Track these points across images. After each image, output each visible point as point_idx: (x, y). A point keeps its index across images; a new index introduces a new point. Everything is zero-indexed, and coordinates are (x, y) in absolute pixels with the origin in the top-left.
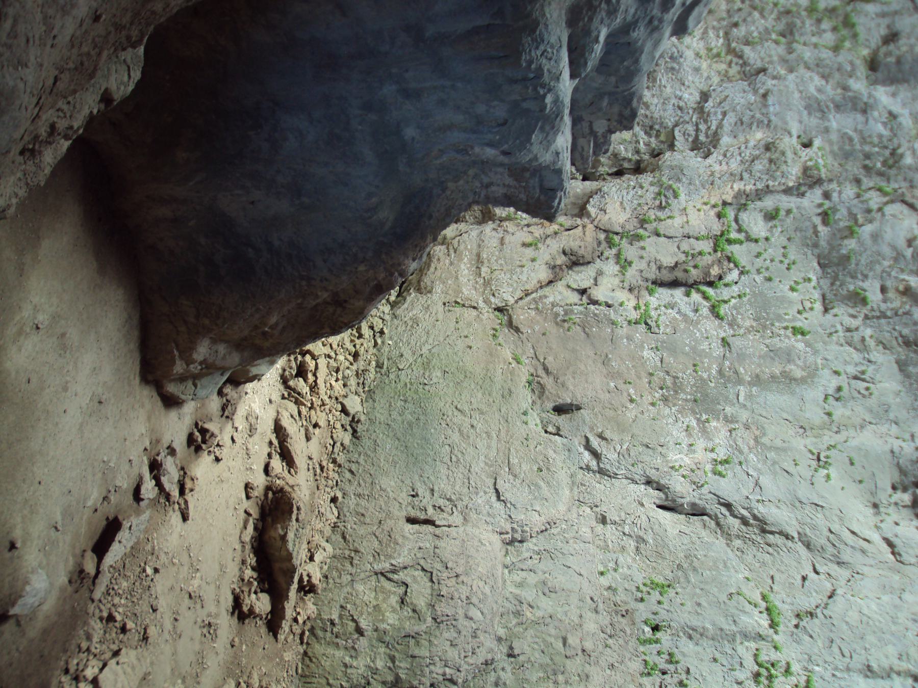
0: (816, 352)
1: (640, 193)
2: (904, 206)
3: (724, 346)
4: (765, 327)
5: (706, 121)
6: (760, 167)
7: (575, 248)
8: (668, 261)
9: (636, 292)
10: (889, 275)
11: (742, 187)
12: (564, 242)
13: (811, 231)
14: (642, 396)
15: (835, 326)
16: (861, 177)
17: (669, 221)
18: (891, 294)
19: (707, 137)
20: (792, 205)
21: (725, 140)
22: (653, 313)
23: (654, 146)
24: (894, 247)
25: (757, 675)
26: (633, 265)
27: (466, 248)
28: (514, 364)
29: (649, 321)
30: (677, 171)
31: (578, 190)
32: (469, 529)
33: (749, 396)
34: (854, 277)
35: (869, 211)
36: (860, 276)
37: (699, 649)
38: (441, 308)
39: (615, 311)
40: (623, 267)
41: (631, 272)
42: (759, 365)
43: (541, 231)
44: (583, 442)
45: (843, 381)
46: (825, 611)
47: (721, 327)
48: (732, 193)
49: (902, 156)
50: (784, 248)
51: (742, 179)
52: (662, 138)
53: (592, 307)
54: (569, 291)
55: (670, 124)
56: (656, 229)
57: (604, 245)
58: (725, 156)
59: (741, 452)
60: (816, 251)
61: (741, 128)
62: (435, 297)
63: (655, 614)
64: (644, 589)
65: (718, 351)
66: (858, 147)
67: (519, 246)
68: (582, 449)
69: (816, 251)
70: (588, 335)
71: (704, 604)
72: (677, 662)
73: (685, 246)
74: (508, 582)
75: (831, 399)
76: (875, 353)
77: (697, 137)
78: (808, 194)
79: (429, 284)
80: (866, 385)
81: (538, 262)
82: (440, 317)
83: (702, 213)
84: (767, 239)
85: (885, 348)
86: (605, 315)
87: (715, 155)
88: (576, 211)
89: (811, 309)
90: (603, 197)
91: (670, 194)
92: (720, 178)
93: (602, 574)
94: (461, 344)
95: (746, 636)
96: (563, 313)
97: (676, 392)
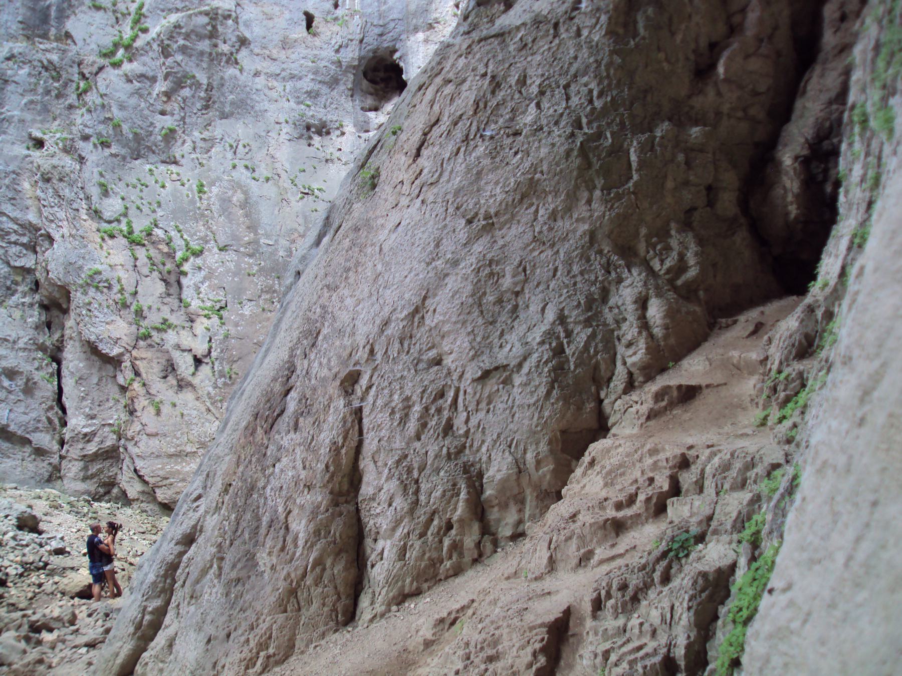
0: (219, 179)
1: (96, 306)
2: (99, 75)
3: (227, 250)
4: (203, 215)
5: (8, 233)
6: (67, 191)
7: (160, 367)
8: (160, 287)
9: (193, 317)
10: (152, 105)
11: (85, 211)
12: (155, 377)
13: (114, 159)
15: (193, 159)
16: (67, 103)
17: (123, 282)
18: (168, 108)
19: (24, 235)
20: (96, 170)
21: (32, 217)
22: (209, 304)
23: (26, 289)
24: (132, 94)
26: (166, 317)
27: (162, 469)
29: (217, 308)
30: (70, 268)
31: (81, 365)
33: (268, 236)
34: (151, 134)
35: (103, 106)
36: (151, 129)
39: (215, 335)
40: (169, 327)
41: (173, 319)
42: (238, 225)
43: (142, 399)
45: (240, 165)
47: (210, 250)
48: (90, 222)
49: (50, 62)
50: (128, 185)
51: (78, 210)
52: (19, 279)
53: (214, 354)
54: (199, 373)
55: (6, 270)
56: (131, 294)
57: (149, 341)
58: (52, 221)
60: (128, 159)
61: (19, 201)
65: (230, 256)
66: (39, 98)
67: (159, 419)
69: (128, 159)
70: (239, 358)
73: (145, 271)
75: (256, 175)
76: (215, 133)
77: (23, 245)
78: (83, 154)
80: (240, 147)
81: (176, 401)
83: (111, 251)
84: (123, 199)
85: (210, 125)
86: (220, 343)
87: (50, 231)
88: (110, 368)
89: (178, 174)
90: (101, 341)
91: (98, 278)
92: (78, 230)
96: (223, 379)
97: (275, 291)
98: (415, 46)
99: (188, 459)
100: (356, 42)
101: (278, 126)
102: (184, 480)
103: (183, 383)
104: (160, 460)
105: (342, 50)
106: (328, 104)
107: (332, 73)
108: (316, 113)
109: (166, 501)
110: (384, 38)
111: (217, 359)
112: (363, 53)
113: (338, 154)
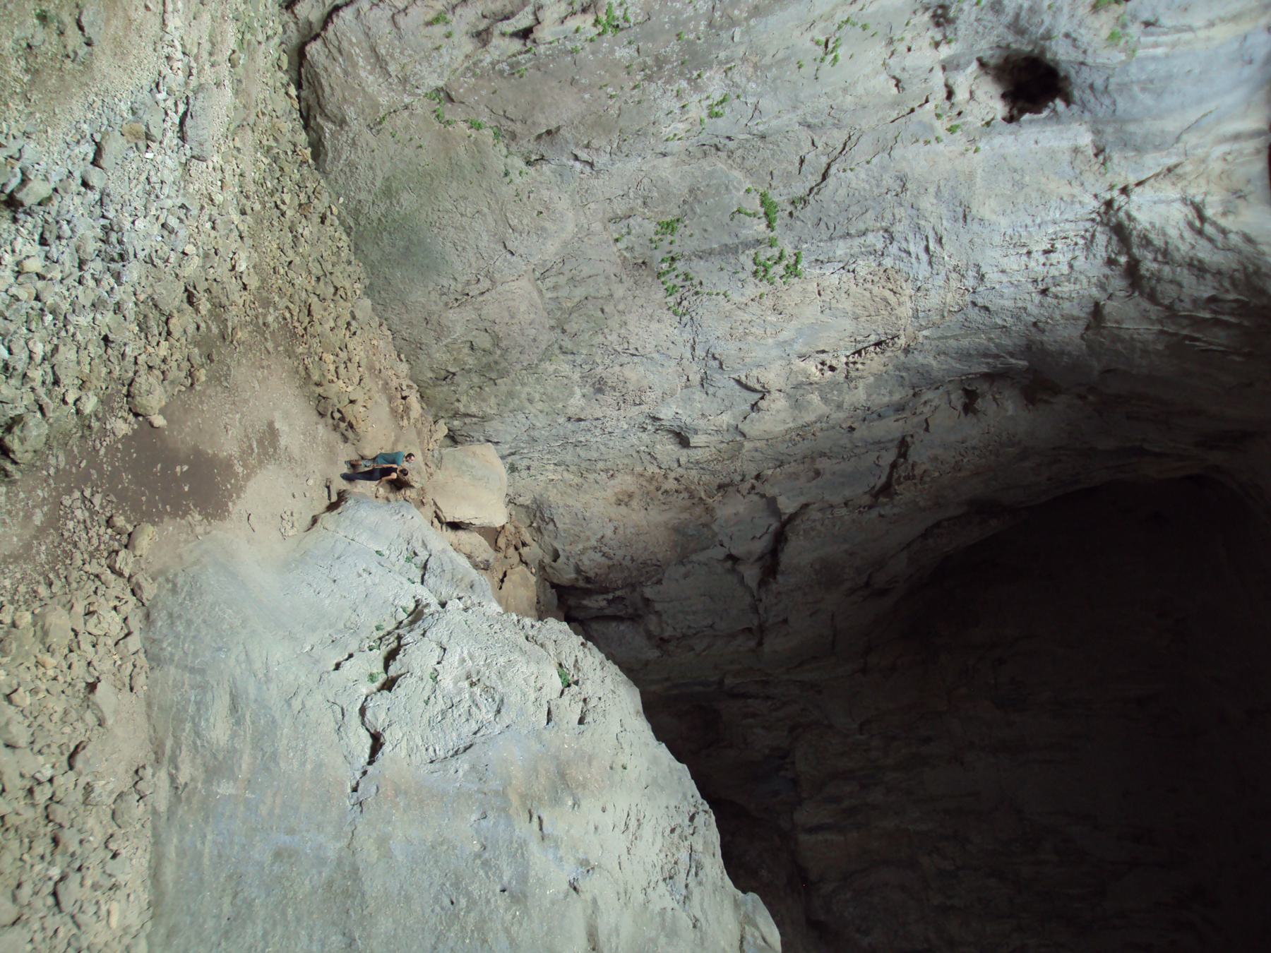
14: (622, 88)
25: (755, 273)
27: (351, 42)
28: (473, 133)
32: (500, 288)
37: (709, 264)
38: (368, 135)
46: (817, 197)
54: (507, 40)
59: (738, 86)
63: (670, 252)
64: (656, 238)
68: (572, 162)
71: (710, 229)
72: (691, 279)
74: (544, 291)
79: (335, 111)
82: (374, 144)
93: (617, 240)
94: (409, 152)
95: (747, 246)
96: (507, 68)
99: (378, 70)
100: (1081, 59)
102: (346, 73)
103: (484, 36)
104: (363, 37)
105: (1069, 41)
106: (983, 23)
107: (1033, 29)
109: (308, 57)
110: (1088, 91)
111: (535, 54)
112: (1064, 65)
113: (902, 48)
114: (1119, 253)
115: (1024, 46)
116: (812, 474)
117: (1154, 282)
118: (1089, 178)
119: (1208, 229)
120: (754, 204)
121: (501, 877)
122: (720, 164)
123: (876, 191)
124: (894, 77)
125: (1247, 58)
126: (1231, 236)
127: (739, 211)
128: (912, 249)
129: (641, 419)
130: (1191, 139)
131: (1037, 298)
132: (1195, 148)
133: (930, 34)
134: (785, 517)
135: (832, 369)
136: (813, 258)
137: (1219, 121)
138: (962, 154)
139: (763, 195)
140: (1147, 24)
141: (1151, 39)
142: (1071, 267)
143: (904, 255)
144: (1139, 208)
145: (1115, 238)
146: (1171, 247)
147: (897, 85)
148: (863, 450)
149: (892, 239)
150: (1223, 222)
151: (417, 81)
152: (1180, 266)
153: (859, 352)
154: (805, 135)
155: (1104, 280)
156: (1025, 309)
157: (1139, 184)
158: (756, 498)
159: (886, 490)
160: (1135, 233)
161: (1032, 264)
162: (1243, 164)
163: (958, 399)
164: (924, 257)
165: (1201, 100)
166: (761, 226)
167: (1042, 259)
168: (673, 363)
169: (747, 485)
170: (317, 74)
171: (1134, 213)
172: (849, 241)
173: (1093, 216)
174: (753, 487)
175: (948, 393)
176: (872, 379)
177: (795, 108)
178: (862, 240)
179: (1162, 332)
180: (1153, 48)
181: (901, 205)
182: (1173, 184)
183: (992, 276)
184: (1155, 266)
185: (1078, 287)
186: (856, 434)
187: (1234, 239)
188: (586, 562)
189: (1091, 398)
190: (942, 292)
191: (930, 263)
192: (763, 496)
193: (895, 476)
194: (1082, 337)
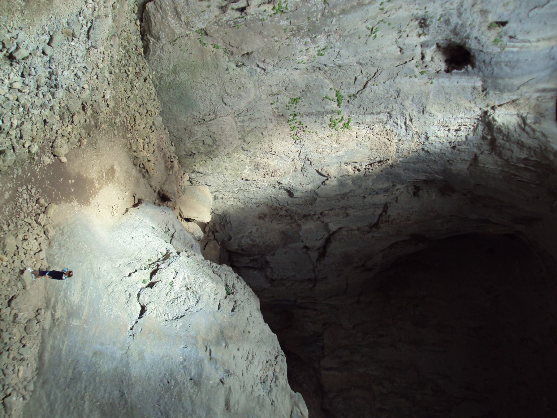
14: (281, 38)
25: (330, 125)
28: (215, 50)
32: (219, 119)
38: (169, 46)
44: (256, 66)
46: (360, 95)
54: (234, 11)
59: (332, 43)
62: (164, 41)
63: (294, 112)
64: (289, 105)
68: (256, 68)
71: (313, 104)
74: (238, 122)
79: (156, 33)
82: (171, 50)
93: (272, 104)
94: (186, 55)
96: (233, 24)
98: (473, 81)
100: (481, 48)
101: (423, 8)
102: (162, 17)
103: (224, 9)
105: (476, 41)
106: (441, 28)
107: (462, 34)
108: (434, 25)
109: (147, 8)
110: (482, 63)
111: (245, 19)
112: (473, 51)
113: (404, 35)
114: (488, 135)
115: (456, 40)
116: (345, 215)
117: (501, 149)
118: (478, 101)
119: (527, 128)
120: (333, 95)
121: (190, 374)
122: (320, 76)
123: (386, 96)
124: (399, 47)
125: (552, 57)
126: (536, 133)
127: (326, 97)
128: (399, 122)
129: (274, 183)
130: (524, 89)
131: (450, 150)
132: (525, 93)
133: (417, 30)
134: (331, 232)
135: (359, 170)
136: (356, 121)
137: (537, 83)
138: (425, 84)
139: (337, 92)
140: (511, 37)
141: (512, 44)
142: (466, 138)
143: (395, 125)
144: (498, 116)
145: (487, 128)
146: (510, 135)
147: (400, 51)
148: (368, 207)
149: (391, 117)
150: (534, 126)
151: (193, 24)
152: (513, 143)
153: (371, 164)
154: (358, 67)
155: (480, 145)
156: (445, 154)
157: (500, 106)
158: (319, 223)
159: (376, 225)
160: (495, 126)
161: (450, 135)
162: (545, 102)
163: (411, 189)
164: (404, 127)
165: (530, 73)
166: (335, 105)
167: (454, 133)
168: (290, 160)
169: (316, 217)
170: (150, 16)
171: (496, 118)
172: (372, 116)
173: (478, 117)
174: (319, 218)
175: (408, 187)
176: (375, 177)
177: (355, 55)
178: (378, 116)
179: (502, 171)
180: (513, 48)
181: (396, 103)
182: (514, 107)
183: (432, 138)
184: (503, 142)
185: (468, 147)
186: (366, 200)
187: (538, 134)
188: (243, 242)
189: (469, 195)
190: (410, 142)
191: (406, 129)
192: (323, 222)
193: (381, 220)
194: (468, 169)
